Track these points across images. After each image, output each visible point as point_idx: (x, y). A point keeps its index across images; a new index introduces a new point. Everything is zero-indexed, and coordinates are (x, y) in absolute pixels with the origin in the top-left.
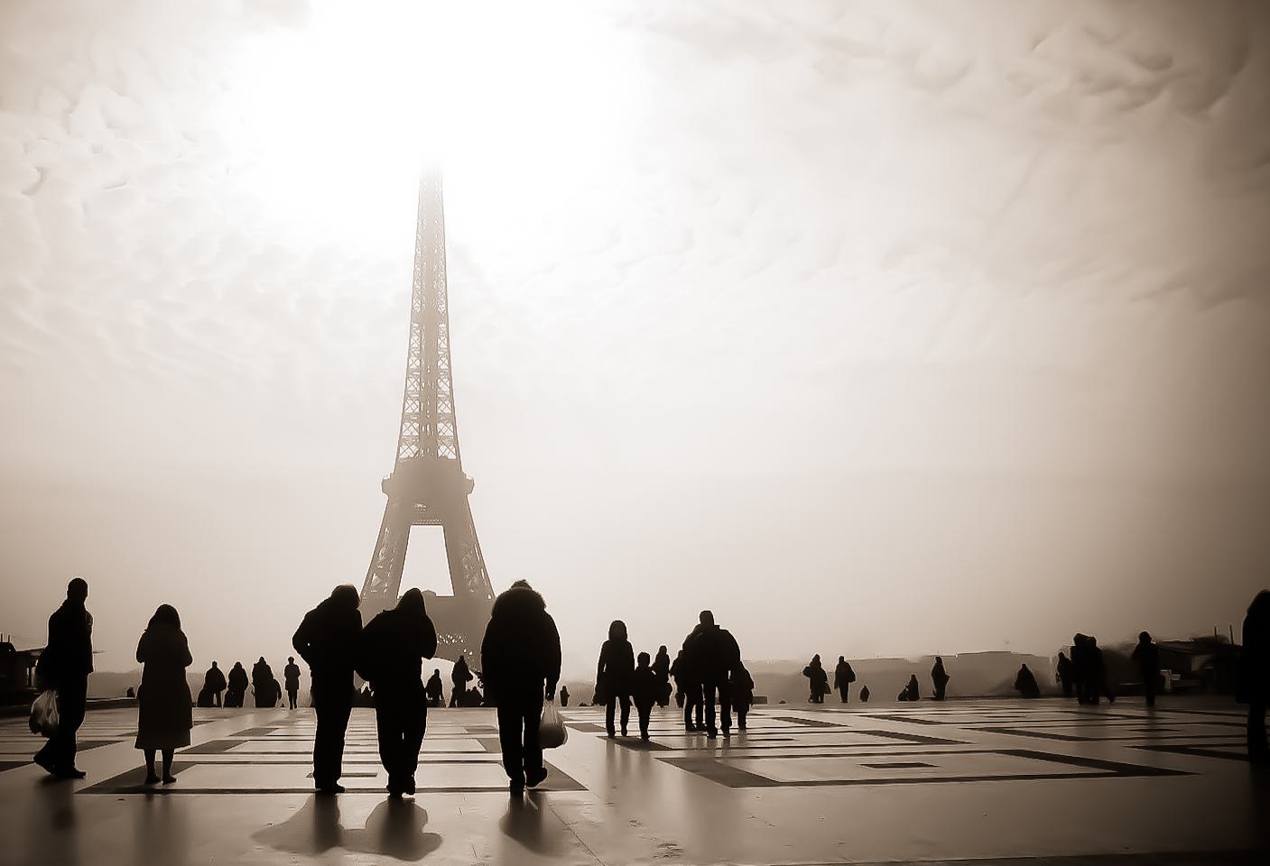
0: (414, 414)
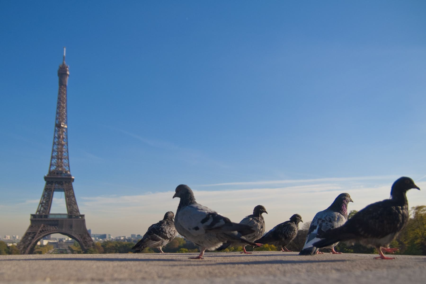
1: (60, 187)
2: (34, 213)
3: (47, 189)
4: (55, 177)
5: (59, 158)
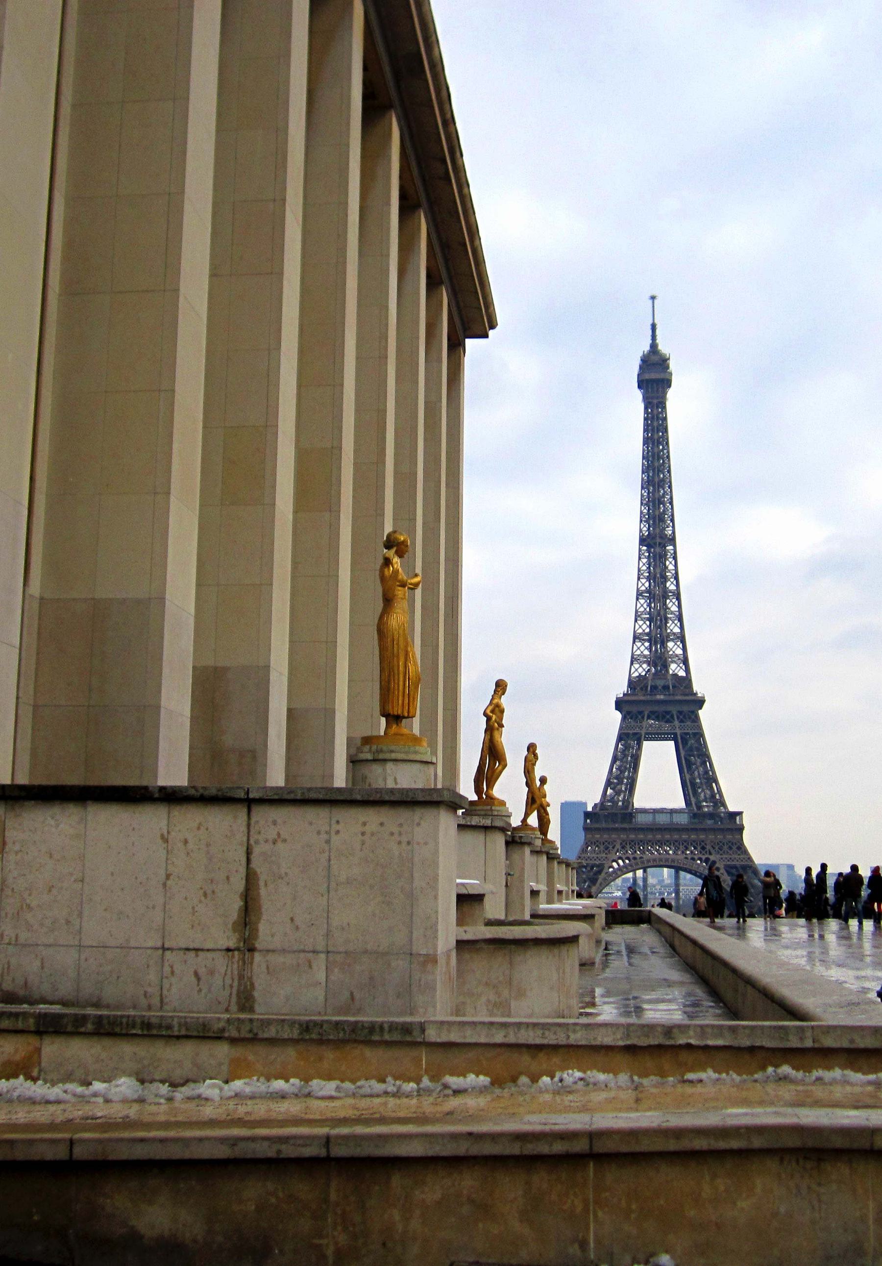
0: (644, 633)
3: (627, 735)
4: (649, 698)
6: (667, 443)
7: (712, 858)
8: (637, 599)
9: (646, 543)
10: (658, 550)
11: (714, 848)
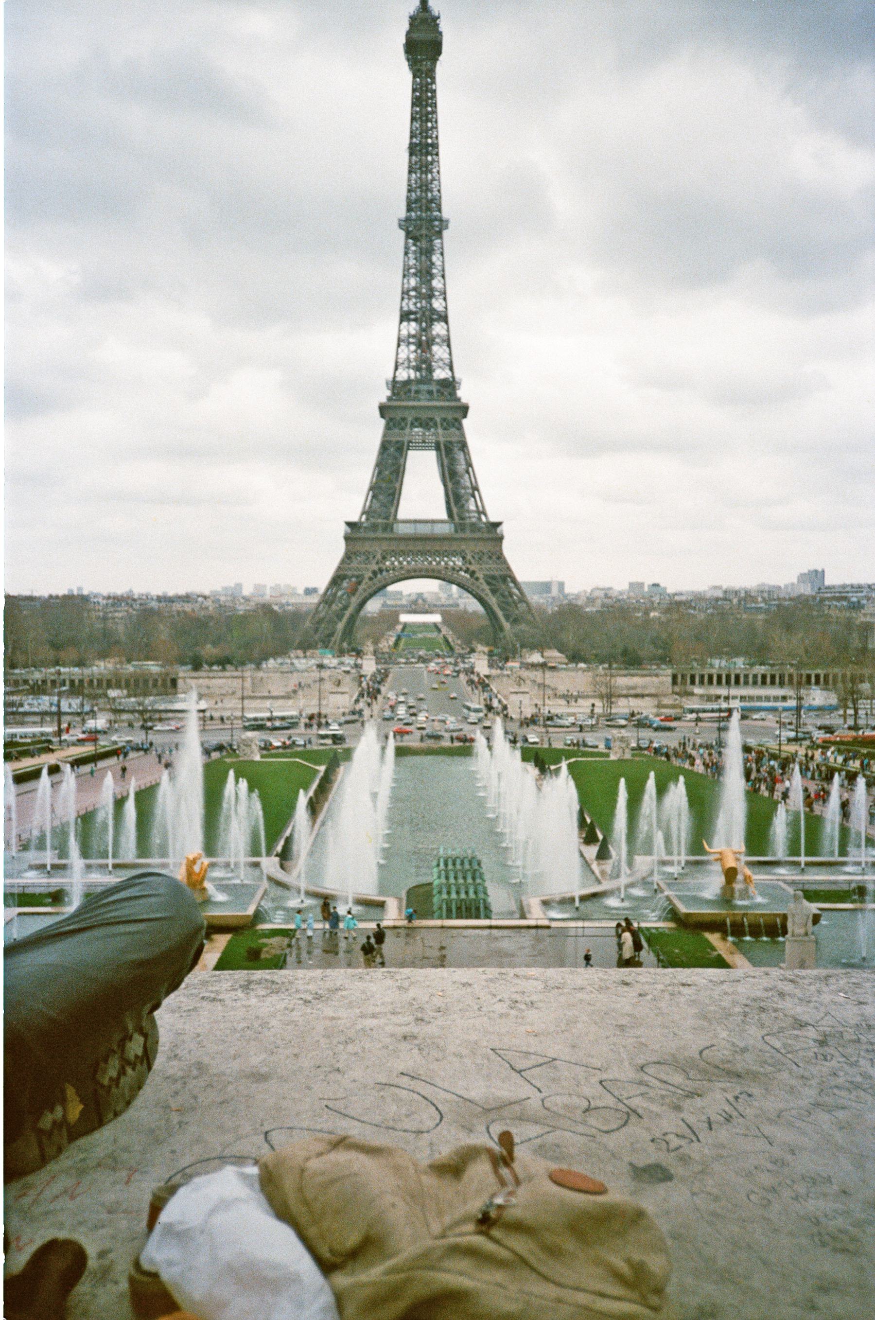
1: (430, 436)
2: (355, 518)
3: (390, 442)
5: (424, 344)
6: (436, 122)
7: (472, 568)
8: (403, 299)
9: (412, 235)
10: (424, 242)
11: (473, 557)
